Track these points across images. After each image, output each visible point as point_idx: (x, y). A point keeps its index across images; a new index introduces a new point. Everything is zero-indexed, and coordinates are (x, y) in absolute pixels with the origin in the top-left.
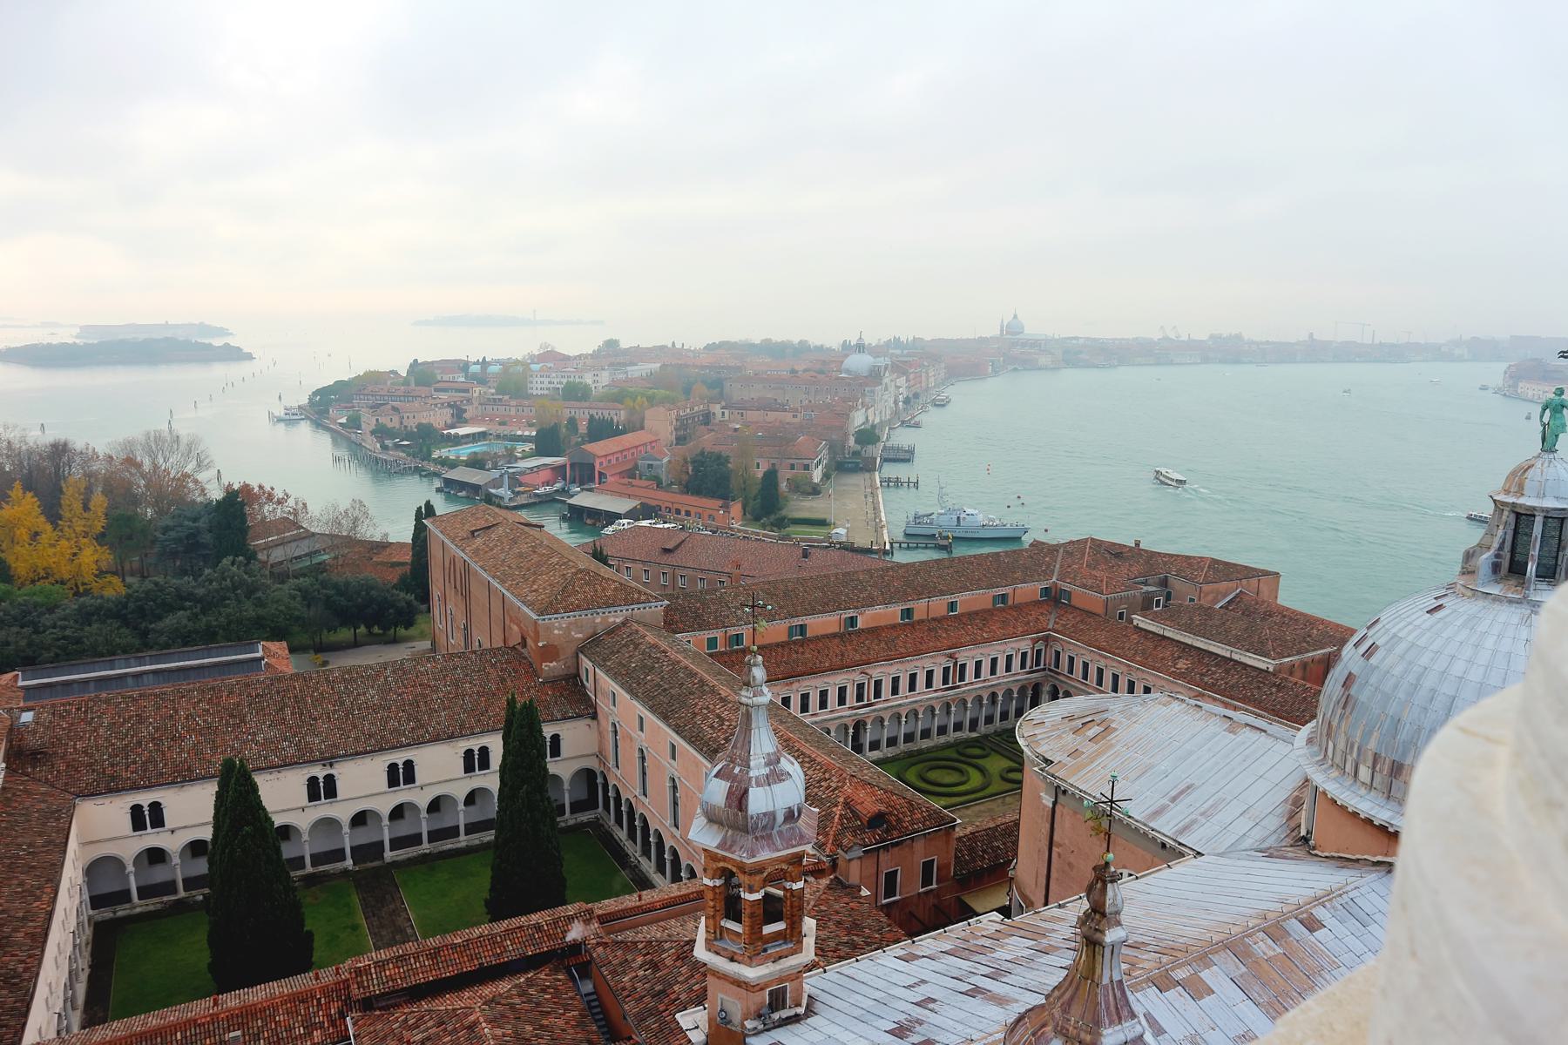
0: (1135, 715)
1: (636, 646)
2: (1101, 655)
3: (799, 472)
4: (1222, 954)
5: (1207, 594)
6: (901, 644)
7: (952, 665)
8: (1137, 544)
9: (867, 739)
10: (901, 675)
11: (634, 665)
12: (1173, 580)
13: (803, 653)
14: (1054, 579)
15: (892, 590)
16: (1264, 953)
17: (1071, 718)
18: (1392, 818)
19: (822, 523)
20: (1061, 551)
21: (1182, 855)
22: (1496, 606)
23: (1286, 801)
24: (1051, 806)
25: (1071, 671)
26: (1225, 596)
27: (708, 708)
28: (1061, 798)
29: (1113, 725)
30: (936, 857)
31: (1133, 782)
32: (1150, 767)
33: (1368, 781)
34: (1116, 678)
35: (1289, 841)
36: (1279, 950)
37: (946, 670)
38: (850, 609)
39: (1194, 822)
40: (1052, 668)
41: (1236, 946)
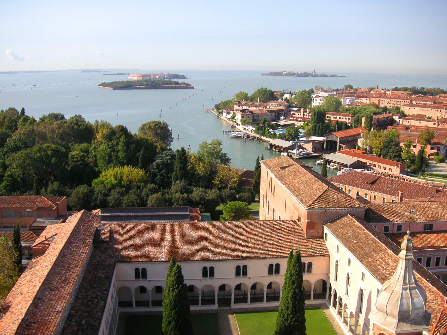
1: (351, 227)
11: (348, 235)
27: (382, 259)
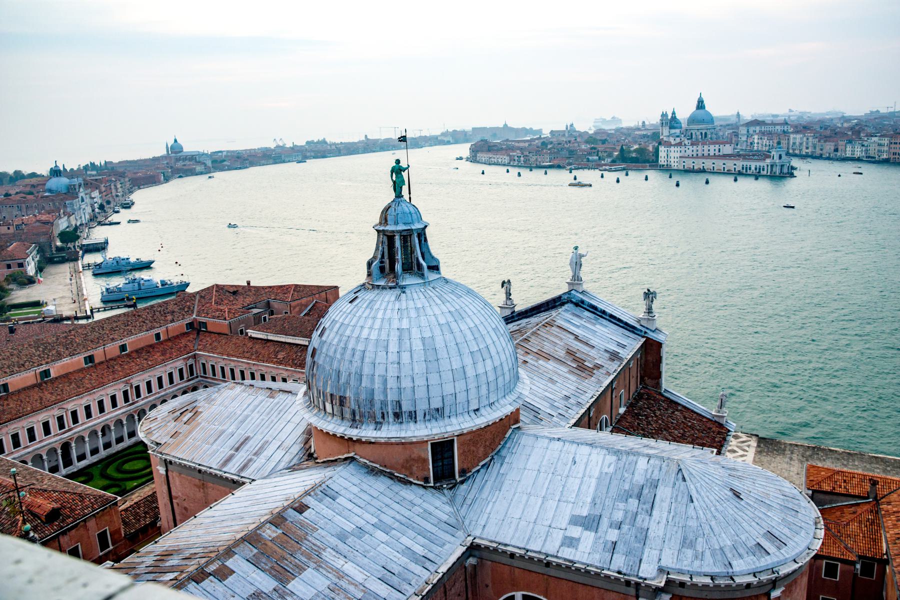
0: (213, 400)
2: (230, 360)
3: (14, 269)
4: (242, 546)
5: (295, 308)
6: (87, 381)
7: (129, 388)
8: (249, 283)
9: (74, 455)
10: (91, 403)
12: (272, 302)
13: (8, 405)
14: (194, 316)
15: (75, 345)
16: (270, 536)
17: (174, 412)
18: (345, 430)
19: (37, 304)
20: (198, 297)
21: (244, 483)
22: (385, 292)
23: (303, 433)
24: (164, 473)
25: (214, 374)
26: (306, 306)
28: (170, 466)
29: (200, 410)
30: (107, 528)
31: (212, 444)
32: (223, 432)
33: (331, 412)
34: (242, 373)
35: (305, 457)
36: (280, 531)
37: (125, 393)
38: (42, 365)
39: (250, 460)
40: (202, 375)
41: (252, 538)
